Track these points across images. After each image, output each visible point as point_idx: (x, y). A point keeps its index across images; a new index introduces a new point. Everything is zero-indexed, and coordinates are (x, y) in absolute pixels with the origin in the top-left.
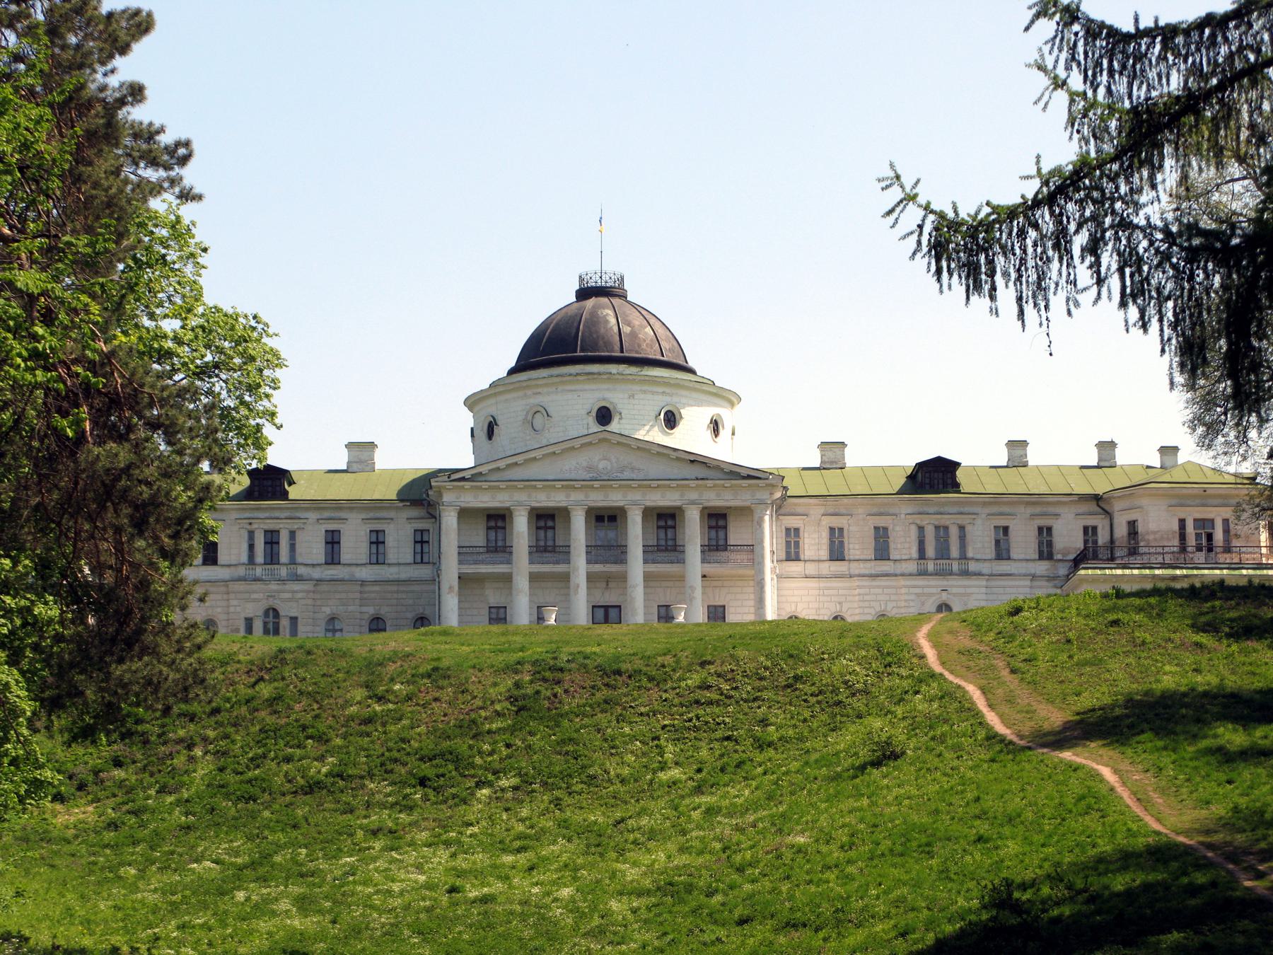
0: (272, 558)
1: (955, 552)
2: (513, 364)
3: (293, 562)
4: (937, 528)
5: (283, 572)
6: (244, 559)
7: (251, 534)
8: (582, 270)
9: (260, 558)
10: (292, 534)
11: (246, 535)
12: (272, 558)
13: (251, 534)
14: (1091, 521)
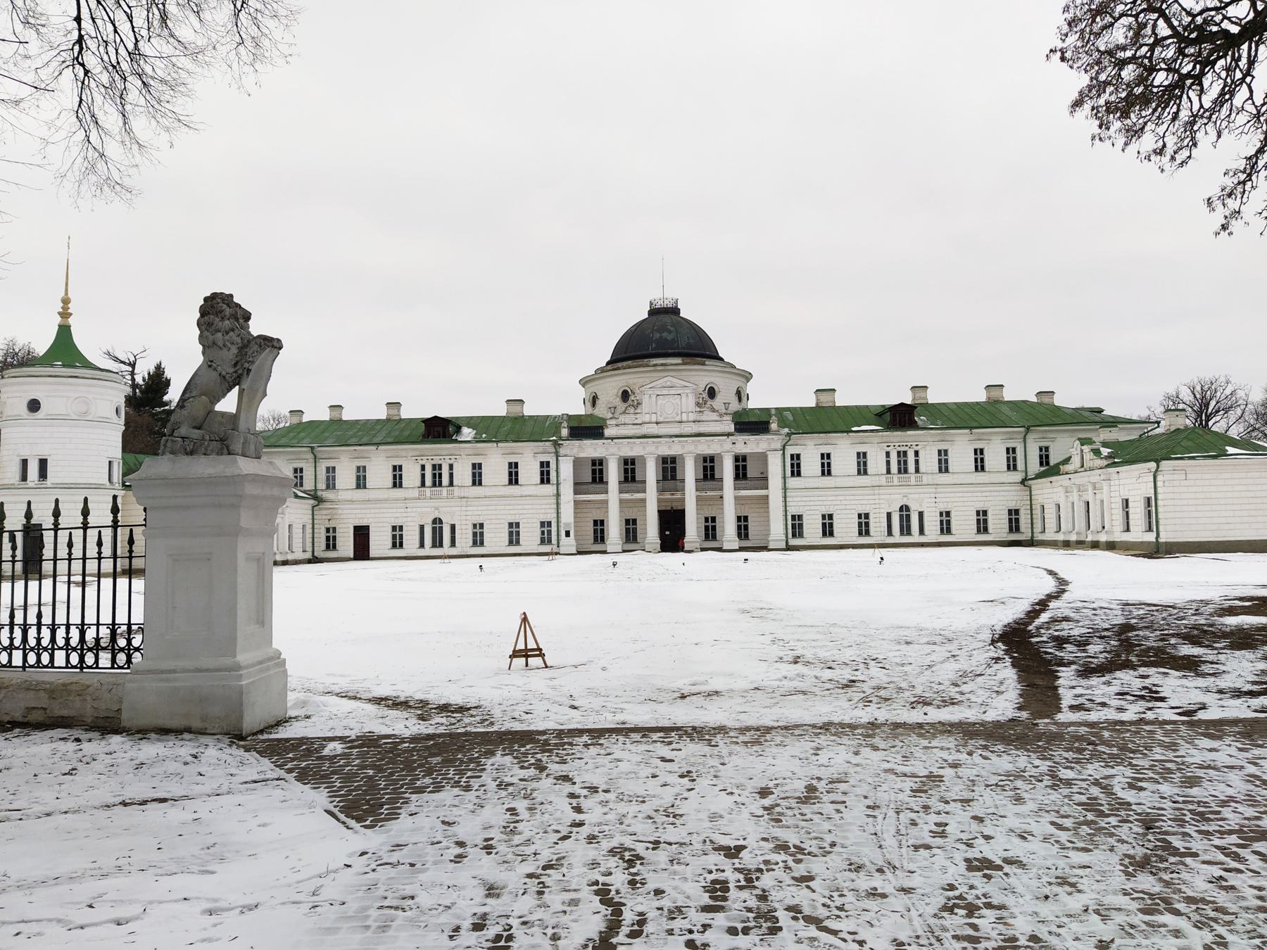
0: (437, 482)
1: (911, 467)
2: (609, 358)
3: (451, 484)
4: (899, 453)
5: (444, 490)
6: (418, 483)
7: (423, 467)
8: (652, 298)
9: (429, 481)
10: (451, 467)
11: (419, 468)
12: (437, 482)
13: (423, 467)
14: (1011, 445)
